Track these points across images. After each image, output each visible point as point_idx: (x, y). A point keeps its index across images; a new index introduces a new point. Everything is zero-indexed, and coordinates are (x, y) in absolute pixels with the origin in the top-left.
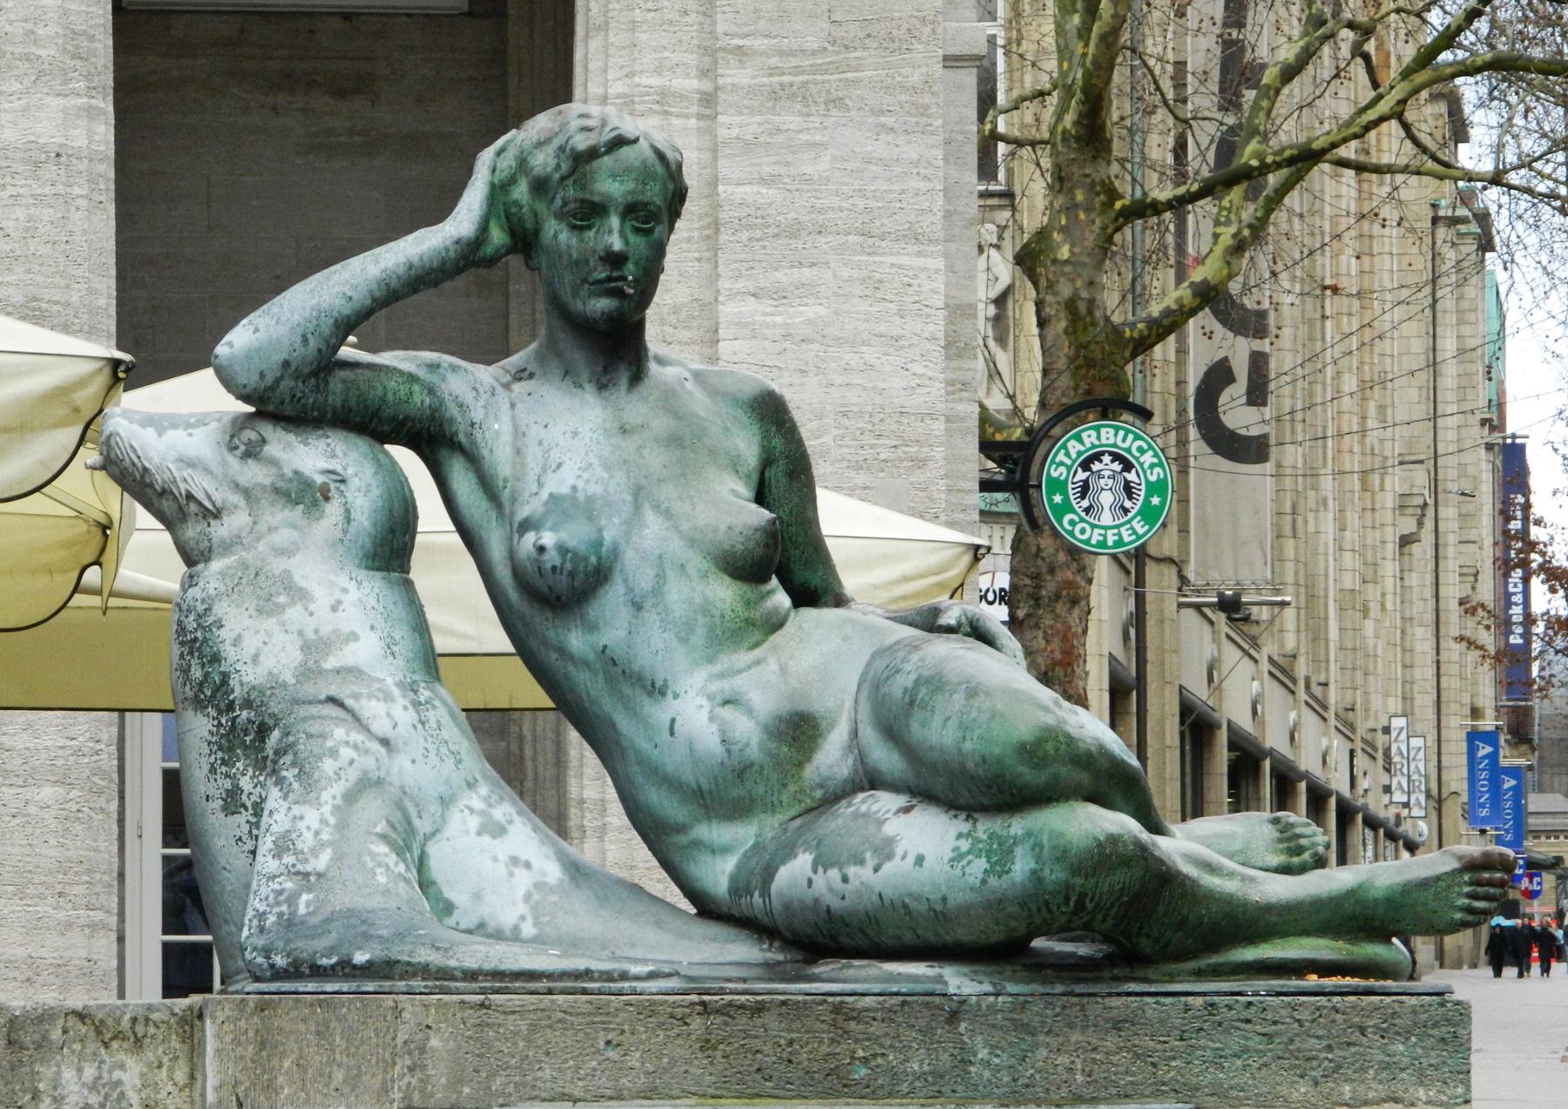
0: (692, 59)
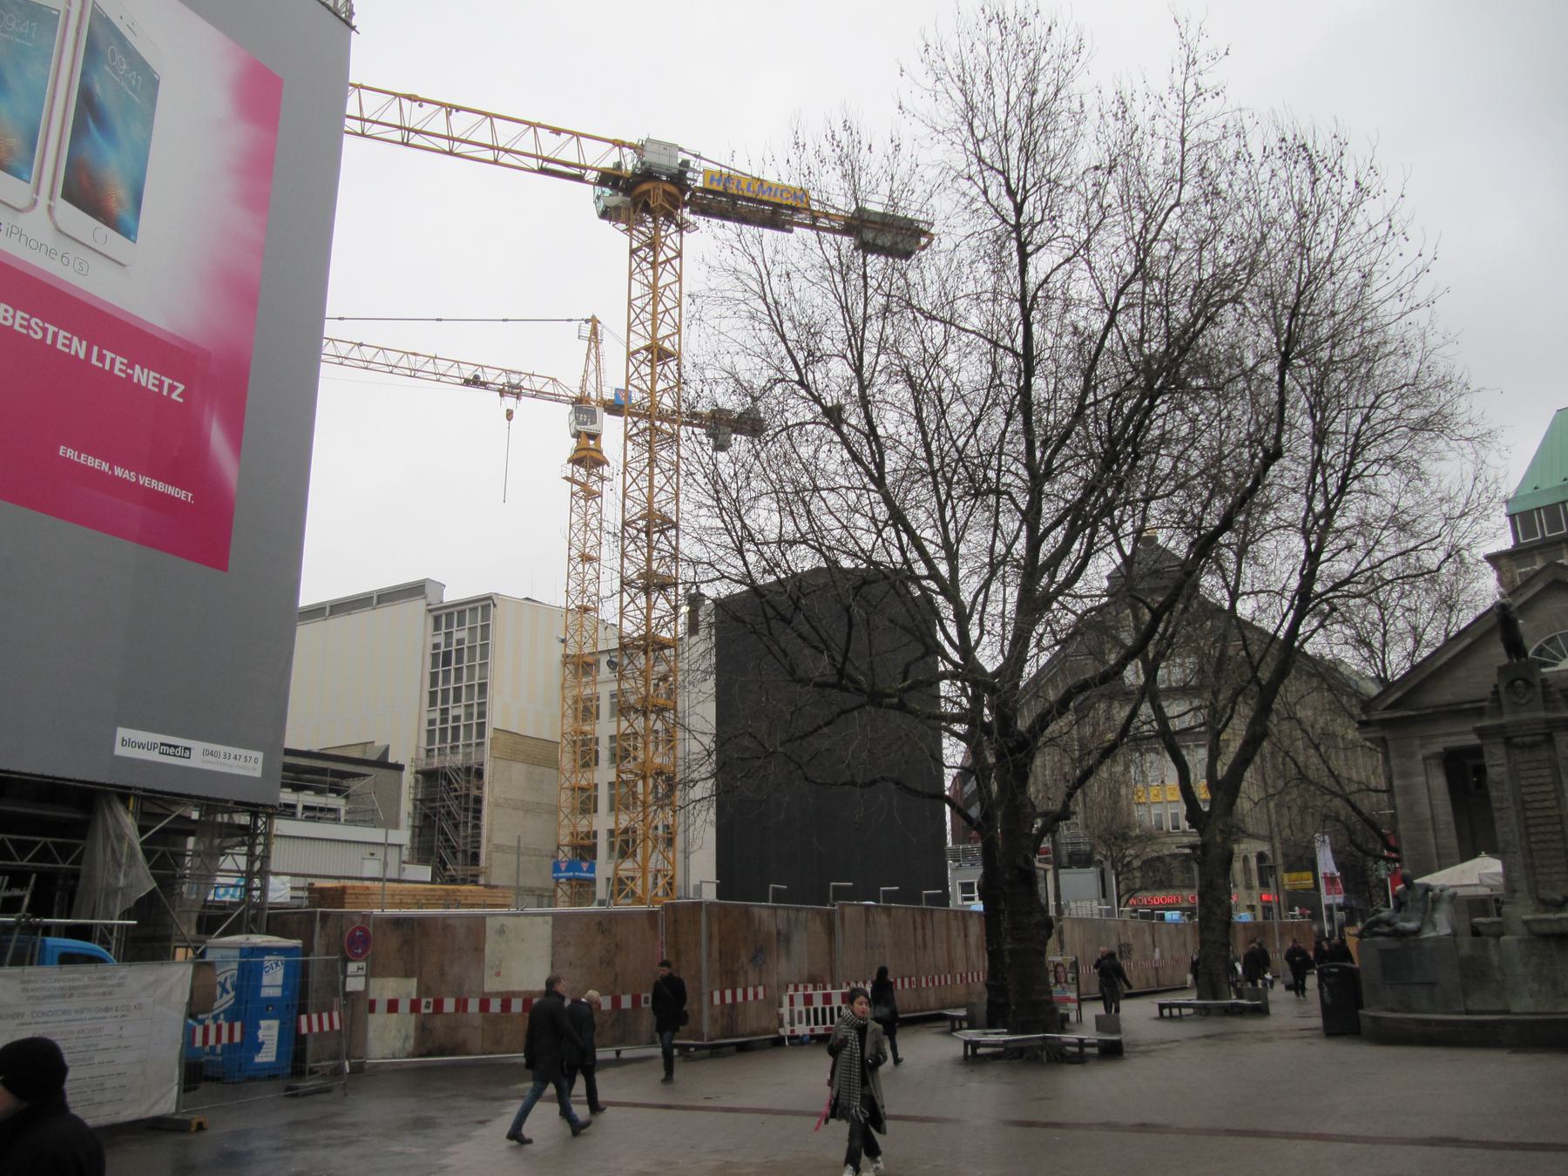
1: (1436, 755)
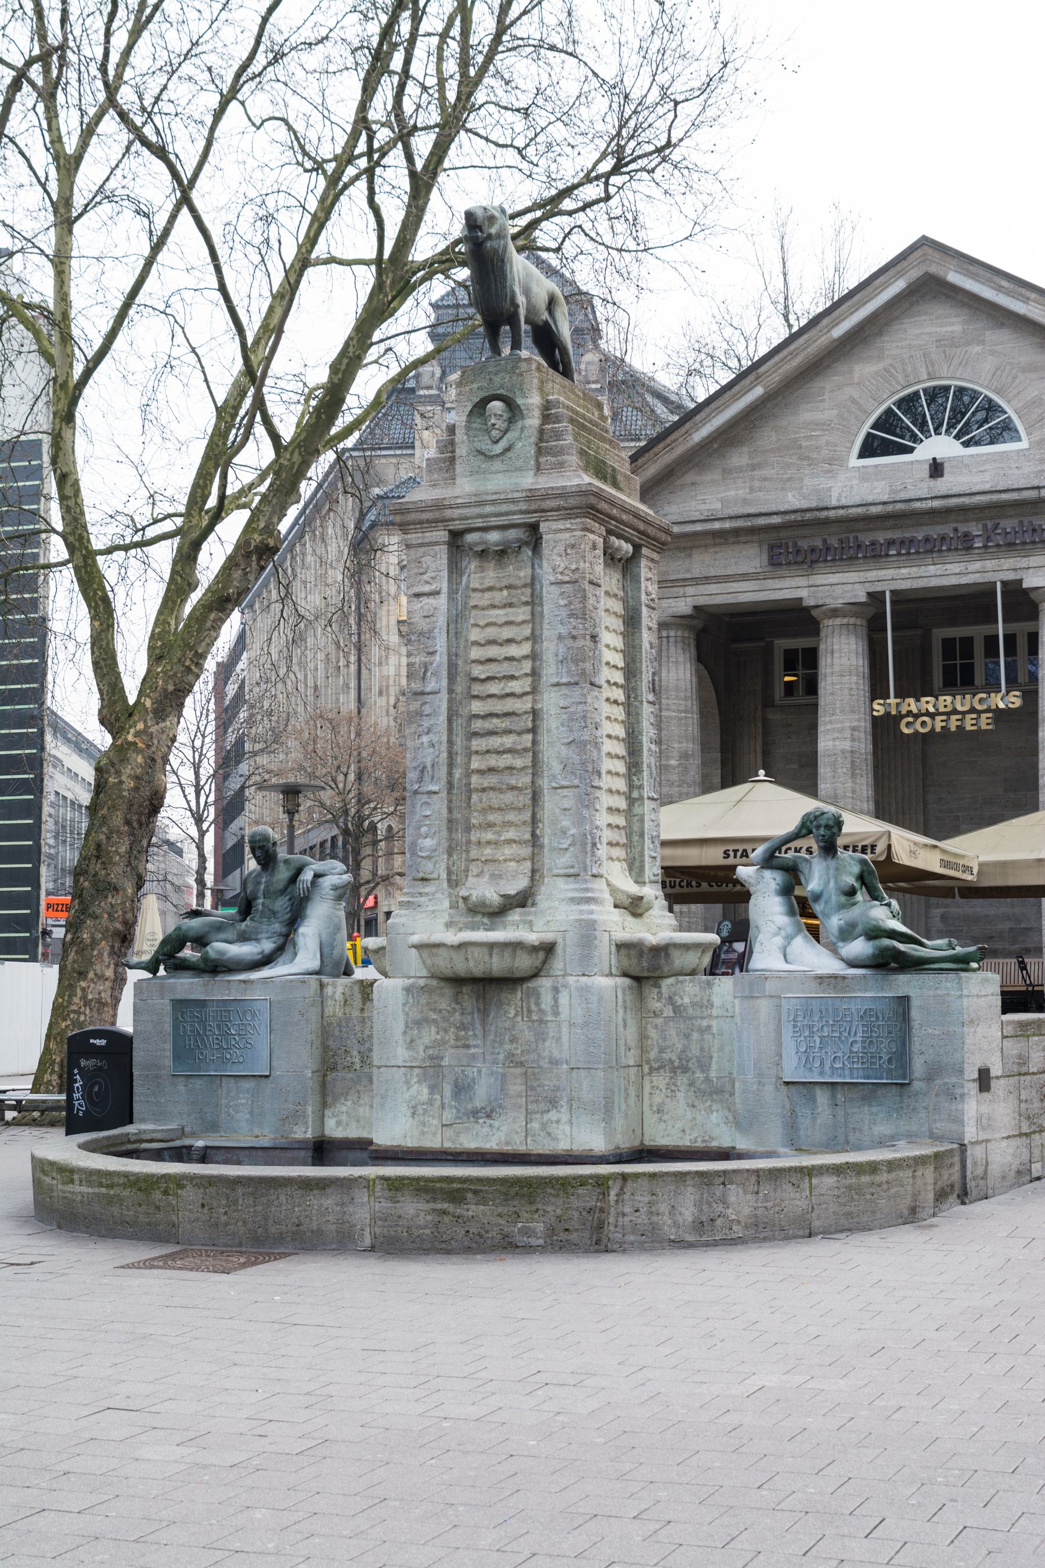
1: (680, 621)
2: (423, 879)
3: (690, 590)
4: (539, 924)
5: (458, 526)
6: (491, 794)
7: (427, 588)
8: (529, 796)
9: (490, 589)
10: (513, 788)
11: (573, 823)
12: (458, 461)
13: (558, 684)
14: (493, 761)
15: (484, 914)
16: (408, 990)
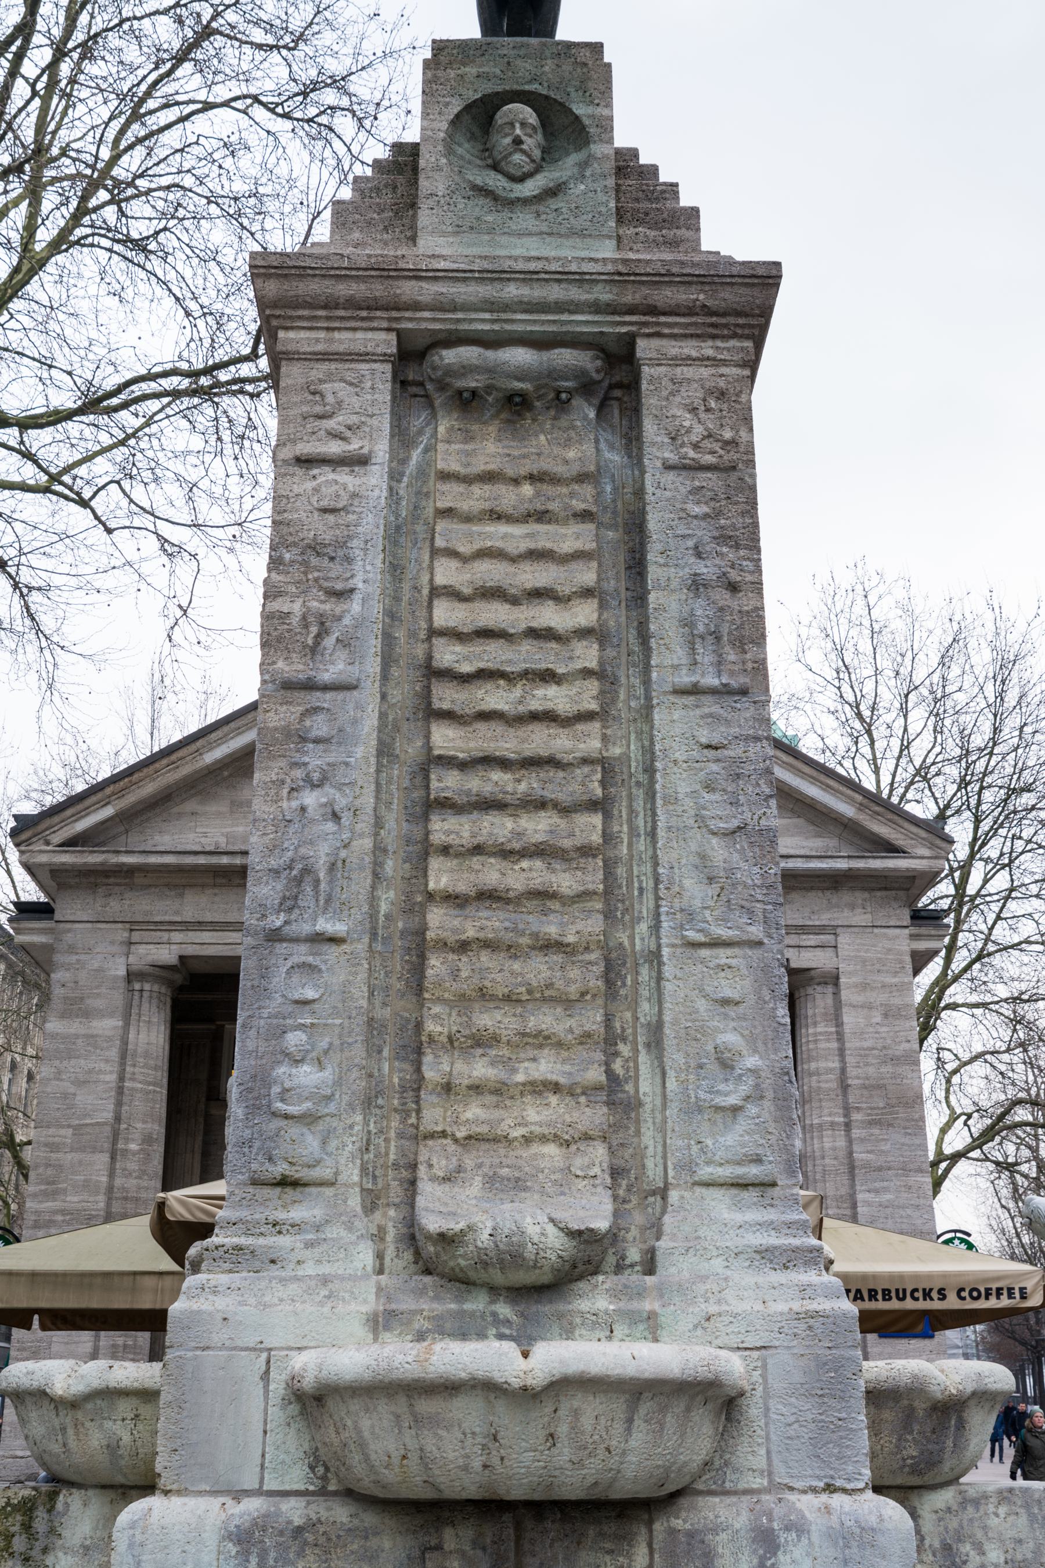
0: (841, 1111)
1: (161, 972)
2: (285, 1183)
3: (177, 937)
4: (679, 1317)
5: (427, 322)
6: (485, 958)
7: (334, 448)
8: (599, 969)
9: (489, 477)
10: (549, 946)
11: (751, 1041)
12: (424, 205)
13: (694, 690)
14: (492, 874)
15: (494, 1291)
16: (244, 1539)
